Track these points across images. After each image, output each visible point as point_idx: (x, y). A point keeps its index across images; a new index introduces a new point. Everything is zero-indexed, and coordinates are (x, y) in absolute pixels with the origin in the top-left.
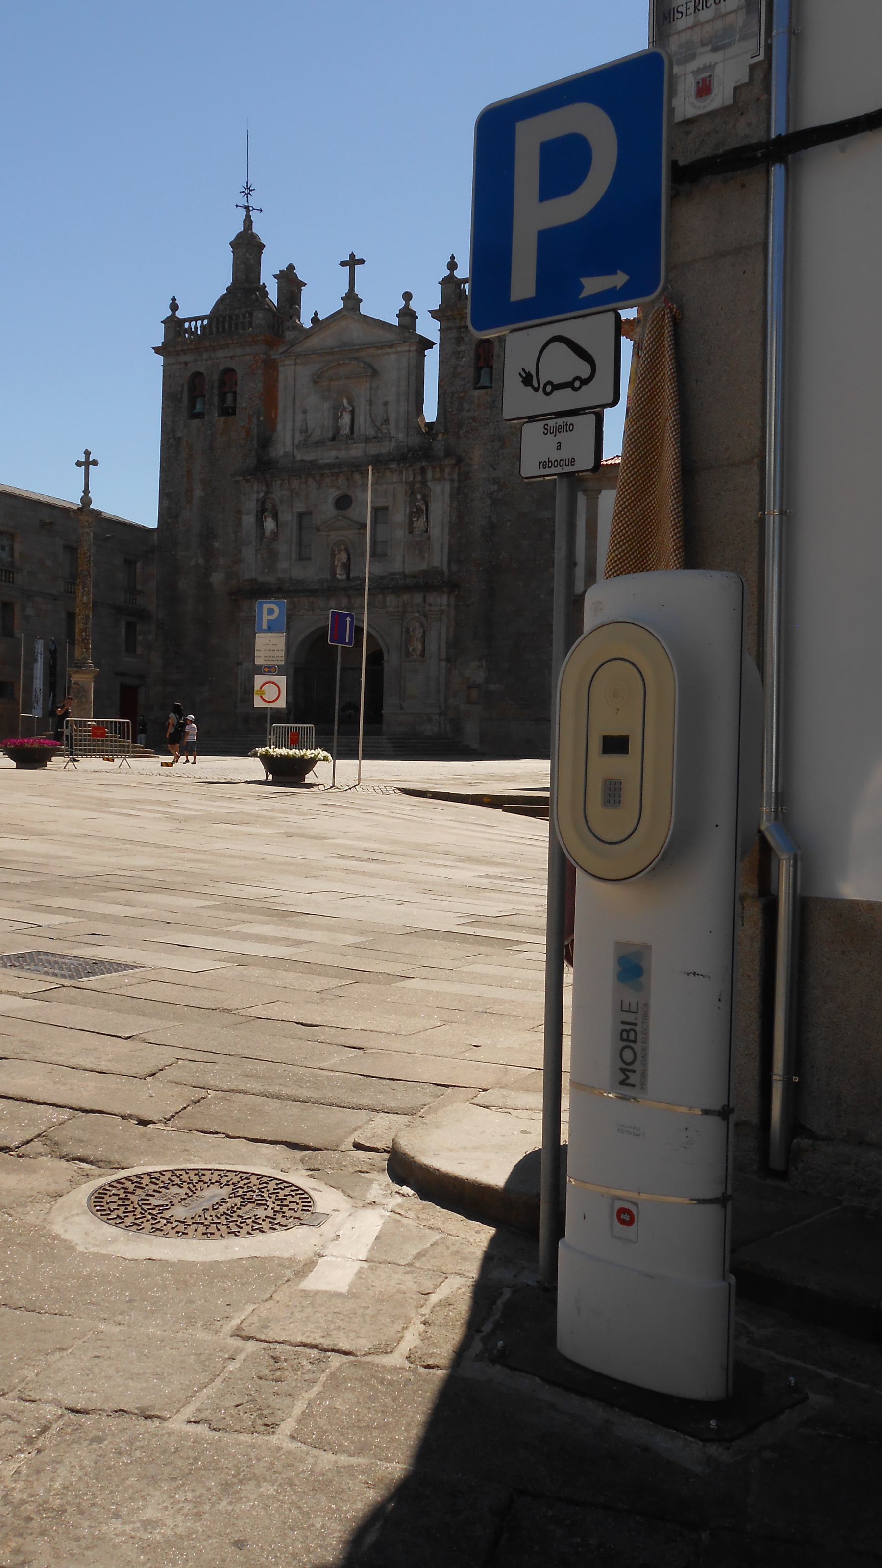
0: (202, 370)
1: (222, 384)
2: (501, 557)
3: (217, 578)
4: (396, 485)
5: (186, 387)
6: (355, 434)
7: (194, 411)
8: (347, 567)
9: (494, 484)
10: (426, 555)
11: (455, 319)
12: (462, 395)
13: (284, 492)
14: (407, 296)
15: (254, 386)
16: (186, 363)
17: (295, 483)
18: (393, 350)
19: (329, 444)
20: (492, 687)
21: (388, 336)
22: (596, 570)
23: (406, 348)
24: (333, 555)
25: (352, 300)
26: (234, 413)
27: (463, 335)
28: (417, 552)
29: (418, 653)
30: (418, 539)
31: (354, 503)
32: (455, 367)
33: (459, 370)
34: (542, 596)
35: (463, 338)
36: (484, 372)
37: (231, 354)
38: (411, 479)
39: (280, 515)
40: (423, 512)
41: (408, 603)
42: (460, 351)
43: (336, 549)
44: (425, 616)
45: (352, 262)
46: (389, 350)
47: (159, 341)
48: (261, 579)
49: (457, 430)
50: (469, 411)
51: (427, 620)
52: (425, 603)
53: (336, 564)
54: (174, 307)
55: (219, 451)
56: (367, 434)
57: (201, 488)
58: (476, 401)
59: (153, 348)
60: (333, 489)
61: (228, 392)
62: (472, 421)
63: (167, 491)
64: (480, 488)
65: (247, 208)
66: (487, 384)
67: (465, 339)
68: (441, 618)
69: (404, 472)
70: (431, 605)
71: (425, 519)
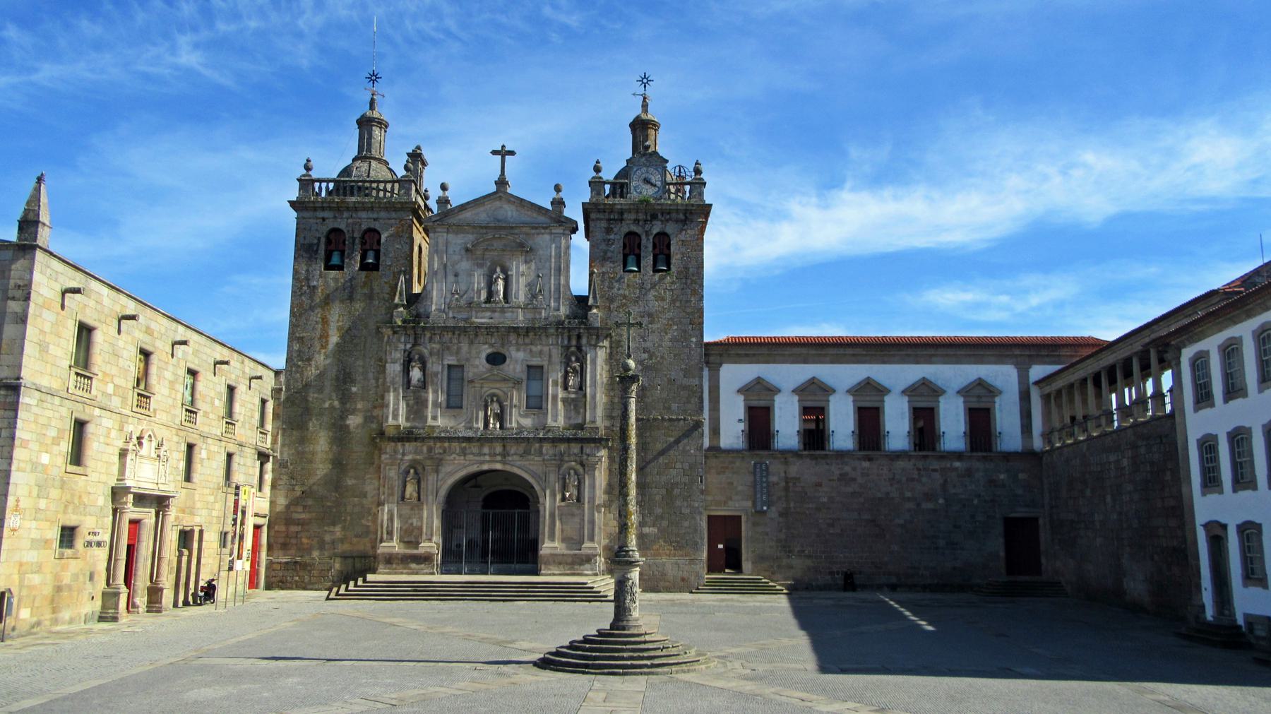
0: (342, 226)
3: (354, 421)
4: (551, 347)
5: (323, 240)
7: (330, 264)
8: (500, 417)
9: (644, 353)
10: (582, 410)
11: (605, 212)
12: (612, 276)
13: (434, 345)
14: (557, 189)
15: (400, 247)
16: (324, 219)
18: (547, 231)
19: (483, 305)
20: (646, 530)
21: (542, 219)
23: (562, 231)
26: (377, 269)
27: (612, 226)
28: (572, 407)
30: (573, 396)
31: (508, 361)
32: (605, 252)
33: (609, 254)
34: (692, 451)
35: (612, 228)
36: (631, 259)
37: (375, 216)
38: (566, 342)
39: (429, 365)
41: (565, 453)
43: (489, 401)
44: (582, 464)
46: (543, 231)
47: (294, 196)
49: (608, 305)
50: (619, 289)
51: (584, 469)
52: (582, 453)
54: (308, 168)
59: (289, 201)
60: (487, 346)
62: (621, 298)
63: (298, 335)
69: (560, 337)
70: (588, 455)
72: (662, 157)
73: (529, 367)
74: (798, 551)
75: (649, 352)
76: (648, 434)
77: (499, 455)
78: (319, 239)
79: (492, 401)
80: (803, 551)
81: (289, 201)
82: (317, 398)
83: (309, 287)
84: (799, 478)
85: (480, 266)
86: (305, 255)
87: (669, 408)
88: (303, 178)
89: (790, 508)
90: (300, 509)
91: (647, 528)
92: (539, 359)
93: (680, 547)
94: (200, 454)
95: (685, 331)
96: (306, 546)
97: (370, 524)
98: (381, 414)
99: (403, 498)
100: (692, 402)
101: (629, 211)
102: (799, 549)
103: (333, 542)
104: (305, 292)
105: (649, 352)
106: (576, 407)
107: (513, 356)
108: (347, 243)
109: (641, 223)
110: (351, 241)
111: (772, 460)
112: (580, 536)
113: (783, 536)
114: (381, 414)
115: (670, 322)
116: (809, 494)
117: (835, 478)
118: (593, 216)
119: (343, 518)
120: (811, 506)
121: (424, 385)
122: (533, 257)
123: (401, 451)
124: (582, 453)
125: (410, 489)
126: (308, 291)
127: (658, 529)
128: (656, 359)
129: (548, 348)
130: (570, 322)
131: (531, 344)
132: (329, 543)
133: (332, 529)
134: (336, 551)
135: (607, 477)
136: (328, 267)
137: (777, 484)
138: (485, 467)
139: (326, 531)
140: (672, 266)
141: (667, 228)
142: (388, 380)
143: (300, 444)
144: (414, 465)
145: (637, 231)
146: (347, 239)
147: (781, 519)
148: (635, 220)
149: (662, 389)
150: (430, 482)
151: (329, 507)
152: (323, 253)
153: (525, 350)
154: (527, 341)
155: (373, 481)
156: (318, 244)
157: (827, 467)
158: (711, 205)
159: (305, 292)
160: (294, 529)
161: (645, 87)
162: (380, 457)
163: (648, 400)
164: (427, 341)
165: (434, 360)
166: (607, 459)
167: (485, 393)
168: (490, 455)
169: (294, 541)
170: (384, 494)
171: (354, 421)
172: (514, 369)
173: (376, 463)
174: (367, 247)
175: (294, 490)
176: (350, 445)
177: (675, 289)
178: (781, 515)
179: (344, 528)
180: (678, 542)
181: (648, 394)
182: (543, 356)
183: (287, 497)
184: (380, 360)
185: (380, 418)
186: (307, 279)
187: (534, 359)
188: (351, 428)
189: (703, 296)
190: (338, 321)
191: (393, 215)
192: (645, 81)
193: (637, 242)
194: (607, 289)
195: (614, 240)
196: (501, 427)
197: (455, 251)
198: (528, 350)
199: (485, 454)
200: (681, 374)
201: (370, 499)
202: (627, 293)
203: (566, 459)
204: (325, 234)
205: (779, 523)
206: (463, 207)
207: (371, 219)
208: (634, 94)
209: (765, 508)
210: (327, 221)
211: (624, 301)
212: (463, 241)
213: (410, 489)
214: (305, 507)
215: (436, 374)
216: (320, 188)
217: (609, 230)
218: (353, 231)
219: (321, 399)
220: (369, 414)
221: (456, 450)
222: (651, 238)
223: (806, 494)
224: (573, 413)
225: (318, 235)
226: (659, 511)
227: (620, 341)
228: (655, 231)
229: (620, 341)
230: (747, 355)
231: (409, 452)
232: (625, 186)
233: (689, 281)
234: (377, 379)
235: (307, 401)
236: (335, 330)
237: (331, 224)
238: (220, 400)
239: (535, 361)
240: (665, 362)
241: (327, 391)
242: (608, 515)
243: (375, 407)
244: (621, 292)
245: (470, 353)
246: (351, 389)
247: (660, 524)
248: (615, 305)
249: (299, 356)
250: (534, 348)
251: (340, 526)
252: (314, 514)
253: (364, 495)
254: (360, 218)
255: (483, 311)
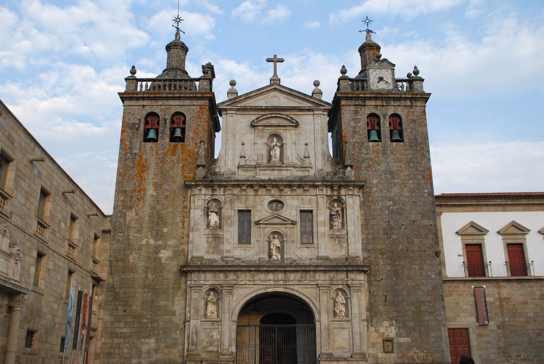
0: (157, 110)
1: (173, 122)
2: (399, 249)
3: (164, 254)
4: (318, 196)
5: (143, 120)
6: (285, 162)
7: (148, 137)
8: (281, 250)
14: (317, 84)
16: (144, 106)
17: (236, 191)
18: (311, 113)
20: (402, 340)
22: (445, 262)
24: (269, 242)
25: (275, 81)
27: (359, 109)
28: (337, 242)
29: (343, 314)
30: (337, 233)
31: (285, 206)
33: (357, 129)
40: (340, 216)
42: (357, 119)
45: (275, 60)
46: (307, 113)
47: (123, 90)
48: (207, 257)
50: (367, 154)
53: (272, 248)
54: (133, 72)
55: (169, 165)
56: (294, 162)
57: (154, 189)
58: (371, 148)
59: (118, 93)
61: (177, 128)
64: (380, 203)
65: (178, 28)
66: (377, 139)
67: (360, 112)
68: (360, 289)
70: (353, 280)
71: (341, 221)
72: (390, 62)
73: (301, 211)
74: (516, 356)
75: (393, 200)
76: (397, 263)
77: (281, 280)
78: (140, 119)
79: (274, 238)
80: (520, 356)
81: (119, 94)
82: (136, 237)
83: (131, 154)
84: (509, 299)
85: (262, 137)
86: (129, 131)
87: (413, 243)
88: (129, 78)
89: (505, 322)
90: (122, 325)
91: (402, 338)
92: (309, 206)
93: (430, 353)
94: (48, 264)
95: (419, 184)
96: (126, 356)
97: (178, 337)
98: (186, 249)
99: (205, 316)
100: (430, 238)
101: (370, 99)
102: (515, 354)
103: (149, 352)
104: (129, 158)
105: (393, 200)
106: (340, 242)
107: (289, 204)
108: (160, 122)
109: (379, 107)
110: (164, 121)
111: (487, 285)
112: (350, 345)
113: (502, 344)
114: (186, 249)
115: (407, 178)
116: (519, 311)
117: (537, 297)
118: (343, 102)
119: (156, 332)
120: (521, 319)
121: (220, 227)
122: (300, 131)
123: (203, 278)
124: (347, 277)
125: (211, 308)
126: (131, 157)
127: (412, 339)
128: (399, 205)
129: (315, 197)
130: (332, 177)
131: (303, 195)
132: (145, 353)
133: (147, 341)
134: (151, 359)
135: (367, 297)
136: (147, 140)
137: (494, 303)
138: (271, 290)
139: (143, 343)
140: (405, 138)
141: (399, 110)
142: (192, 222)
143: (122, 273)
144: (213, 289)
145: (376, 113)
146: (160, 119)
147: (499, 331)
148: (375, 106)
149: (405, 229)
150: (226, 303)
151: (144, 322)
152: (142, 129)
153: (298, 199)
154: (299, 191)
155: (180, 302)
156: (139, 125)
157: (530, 289)
158: (430, 94)
159: (129, 158)
160: (116, 341)
161: (368, 25)
162: (186, 283)
163: (394, 237)
164: (222, 193)
165: (228, 207)
166: (366, 283)
167: (268, 232)
168: (275, 281)
169: (117, 351)
170: (190, 312)
171: (164, 254)
172: (290, 213)
173: (183, 286)
174: (175, 125)
175: (117, 309)
176: (162, 274)
177: (409, 154)
178: (499, 327)
179: (157, 341)
180: (429, 349)
181: (395, 232)
182: (312, 203)
183: (111, 315)
184: (185, 207)
185: (186, 253)
186: (131, 148)
187: (305, 206)
188: (163, 261)
189: (430, 159)
190: (153, 179)
191: (195, 102)
192: (367, 21)
193: (376, 121)
194: (356, 154)
195: (360, 119)
196: (282, 257)
197: (242, 127)
198: (301, 199)
199: (270, 280)
200: (419, 217)
201: (178, 317)
202: (372, 156)
203: (335, 283)
204: (144, 116)
205: (498, 334)
206: (247, 96)
207: (178, 105)
208: (360, 31)
209: (486, 322)
210: (146, 107)
211: (371, 163)
212: (248, 120)
213: (211, 308)
214: (126, 323)
215: (230, 218)
216: (141, 86)
217: (356, 112)
218: (165, 115)
219: (140, 238)
220: (176, 249)
221: (247, 277)
222: (387, 117)
223: (516, 310)
224: (337, 247)
225: (139, 117)
226: (411, 324)
227: (370, 192)
228: (390, 114)
229: (370, 192)
230: (460, 206)
231: (209, 279)
232: (365, 83)
233: (418, 149)
234: (183, 223)
235: (129, 239)
236: (152, 186)
237: (148, 110)
238: (66, 224)
239: (307, 207)
240: (406, 208)
241: (145, 230)
242: (370, 328)
243: (182, 244)
244: (369, 156)
245: (255, 201)
246: (162, 230)
247: (413, 335)
248: (364, 166)
249: (123, 205)
250: (304, 197)
251: (154, 338)
252: (133, 329)
253: (174, 313)
254: (171, 106)
255: (264, 170)
